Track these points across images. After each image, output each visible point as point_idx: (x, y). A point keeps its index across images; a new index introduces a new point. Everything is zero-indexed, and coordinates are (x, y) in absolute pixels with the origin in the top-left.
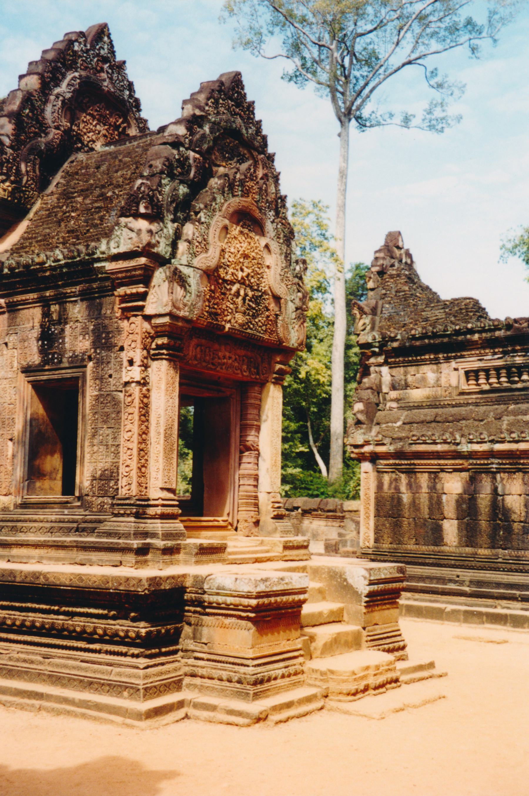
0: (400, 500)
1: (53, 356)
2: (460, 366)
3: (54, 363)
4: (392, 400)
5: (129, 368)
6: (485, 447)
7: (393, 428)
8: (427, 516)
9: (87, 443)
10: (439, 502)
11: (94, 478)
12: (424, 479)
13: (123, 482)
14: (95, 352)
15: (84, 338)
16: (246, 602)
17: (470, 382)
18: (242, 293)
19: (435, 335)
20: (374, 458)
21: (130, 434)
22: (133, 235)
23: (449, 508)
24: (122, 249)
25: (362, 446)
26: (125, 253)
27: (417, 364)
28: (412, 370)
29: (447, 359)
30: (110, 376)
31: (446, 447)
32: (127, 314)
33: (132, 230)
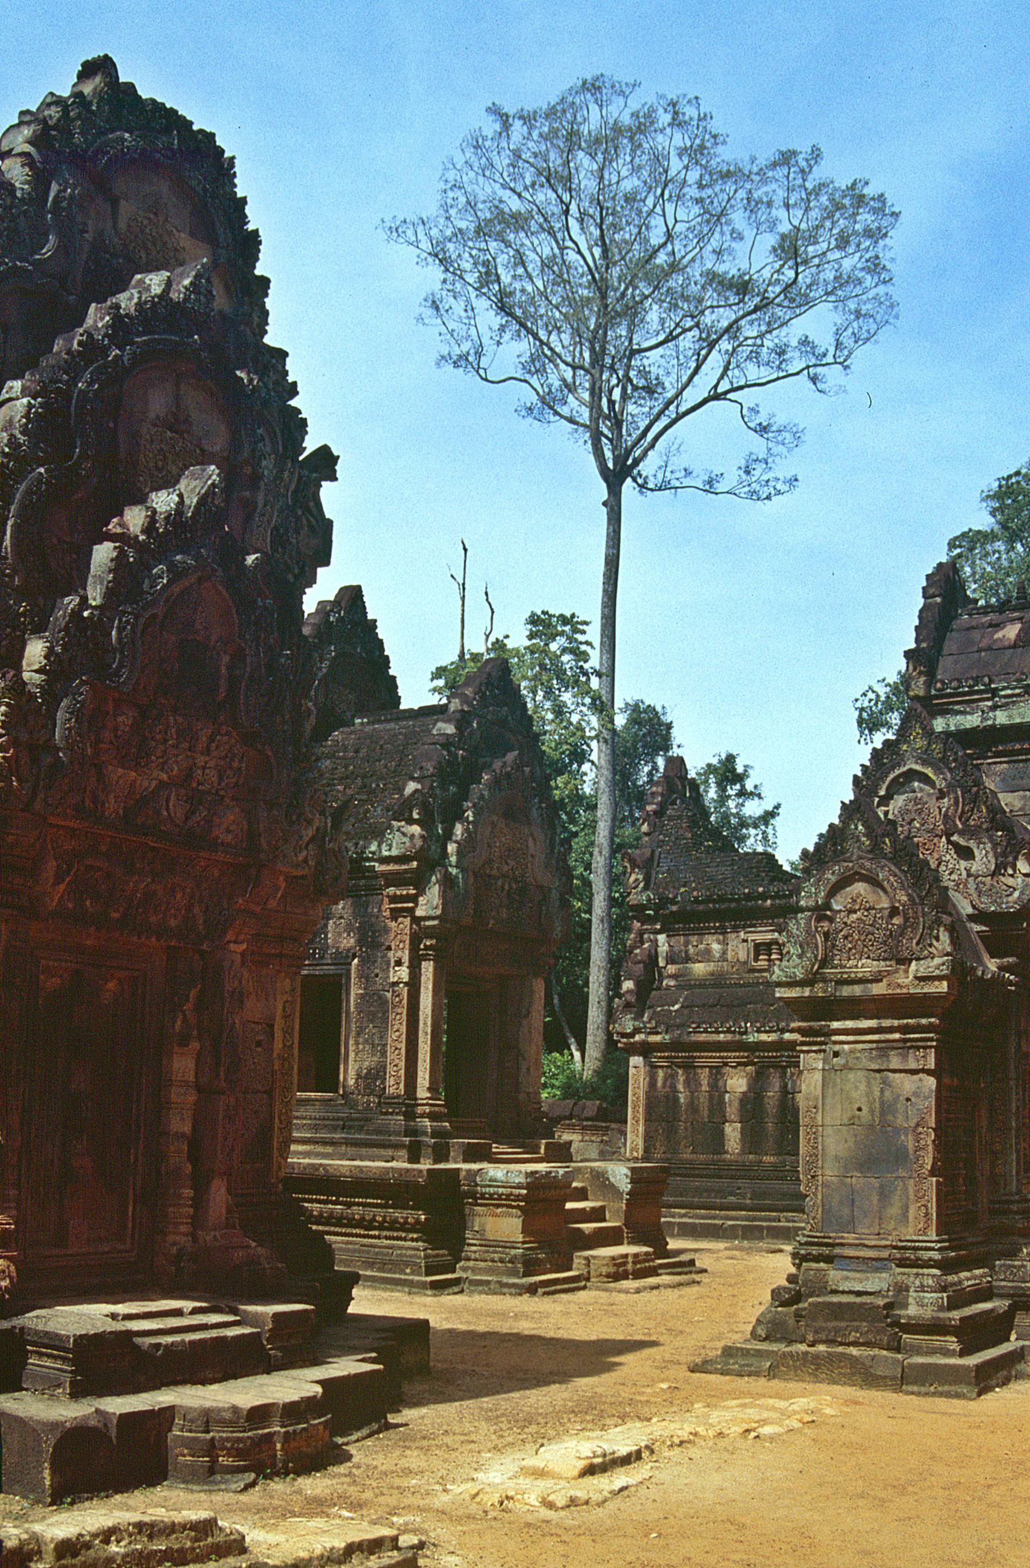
0: (676, 1100)
1: (314, 951)
2: (751, 937)
3: (315, 958)
4: (670, 976)
5: (397, 968)
6: (773, 1037)
7: (671, 1012)
8: (706, 1120)
9: (351, 1042)
10: (721, 1102)
11: (359, 1076)
12: (704, 1076)
13: (390, 1081)
14: (361, 950)
15: (349, 935)
16: (517, 1191)
17: (761, 957)
18: (507, 887)
19: (721, 899)
20: (645, 1050)
21: (397, 1034)
22: (406, 840)
23: (732, 1111)
24: (394, 852)
25: (632, 1035)
26: (397, 857)
27: (701, 933)
28: (694, 939)
29: (735, 929)
30: (377, 975)
31: (729, 1037)
32: (395, 914)
33: (404, 834)
